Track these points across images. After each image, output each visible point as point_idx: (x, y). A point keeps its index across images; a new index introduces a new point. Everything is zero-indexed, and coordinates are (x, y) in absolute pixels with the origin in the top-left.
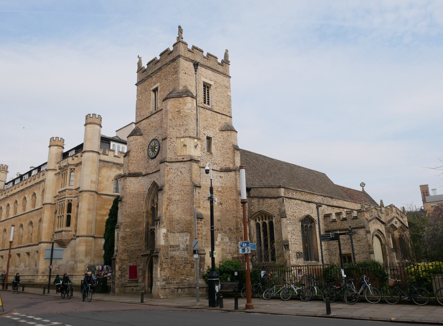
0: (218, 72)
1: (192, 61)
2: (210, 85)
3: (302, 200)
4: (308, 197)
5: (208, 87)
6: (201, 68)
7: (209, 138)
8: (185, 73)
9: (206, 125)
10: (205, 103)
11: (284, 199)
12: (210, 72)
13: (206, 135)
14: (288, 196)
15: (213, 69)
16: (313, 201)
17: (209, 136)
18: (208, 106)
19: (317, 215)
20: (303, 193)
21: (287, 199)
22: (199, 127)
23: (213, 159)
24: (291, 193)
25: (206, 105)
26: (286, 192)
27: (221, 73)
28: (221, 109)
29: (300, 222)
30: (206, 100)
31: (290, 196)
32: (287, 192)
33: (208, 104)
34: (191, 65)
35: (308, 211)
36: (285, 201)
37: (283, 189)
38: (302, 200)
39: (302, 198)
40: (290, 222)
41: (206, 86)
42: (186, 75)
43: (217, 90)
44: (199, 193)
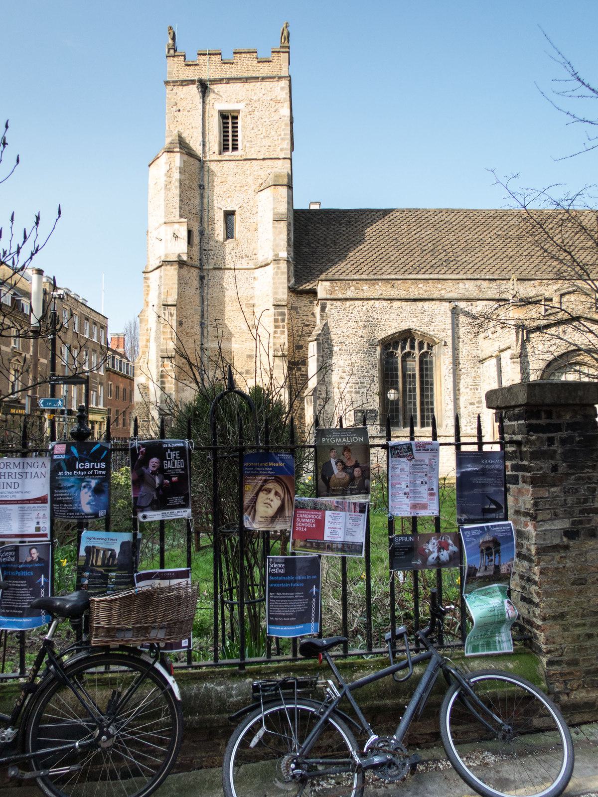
0: (256, 79)
1: (192, 82)
2: (238, 111)
3: (391, 300)
4: (415, 291)
5: (236, 118)
6: (215, 86)
7: (229, 215)
8: (179, 111)
9: (225, 190)
10: (224, 148)
11: (328, 303)
12: (236, 87)
13: (224, 209)
14: (340, 296)
15: (240, 79)
16: (435, 296)
17: (229, 209)
18: (235, 153)
19: (449, 327)
20: (399, 282)
21: (339, 303)
22: (206, 200)
23: (240, 249)
24: (352, 288)
25: (228, 154)
26: (337, 288)
27: (263, 78)
28: (263, 150)
29: (378, 348)
30: (229, 141)
31: (349, 294)
32: (340, 287)
33: (235, 148)
34: (194, 89)
35: (415, 319)
36: (328, 307)
37: (327, 284)
38: (391, 300)
39: (393, 293)
40: (340, 350)
41: (228, 119)
42: (181, 113)
43: (252, 116)
44: (171, 315)
